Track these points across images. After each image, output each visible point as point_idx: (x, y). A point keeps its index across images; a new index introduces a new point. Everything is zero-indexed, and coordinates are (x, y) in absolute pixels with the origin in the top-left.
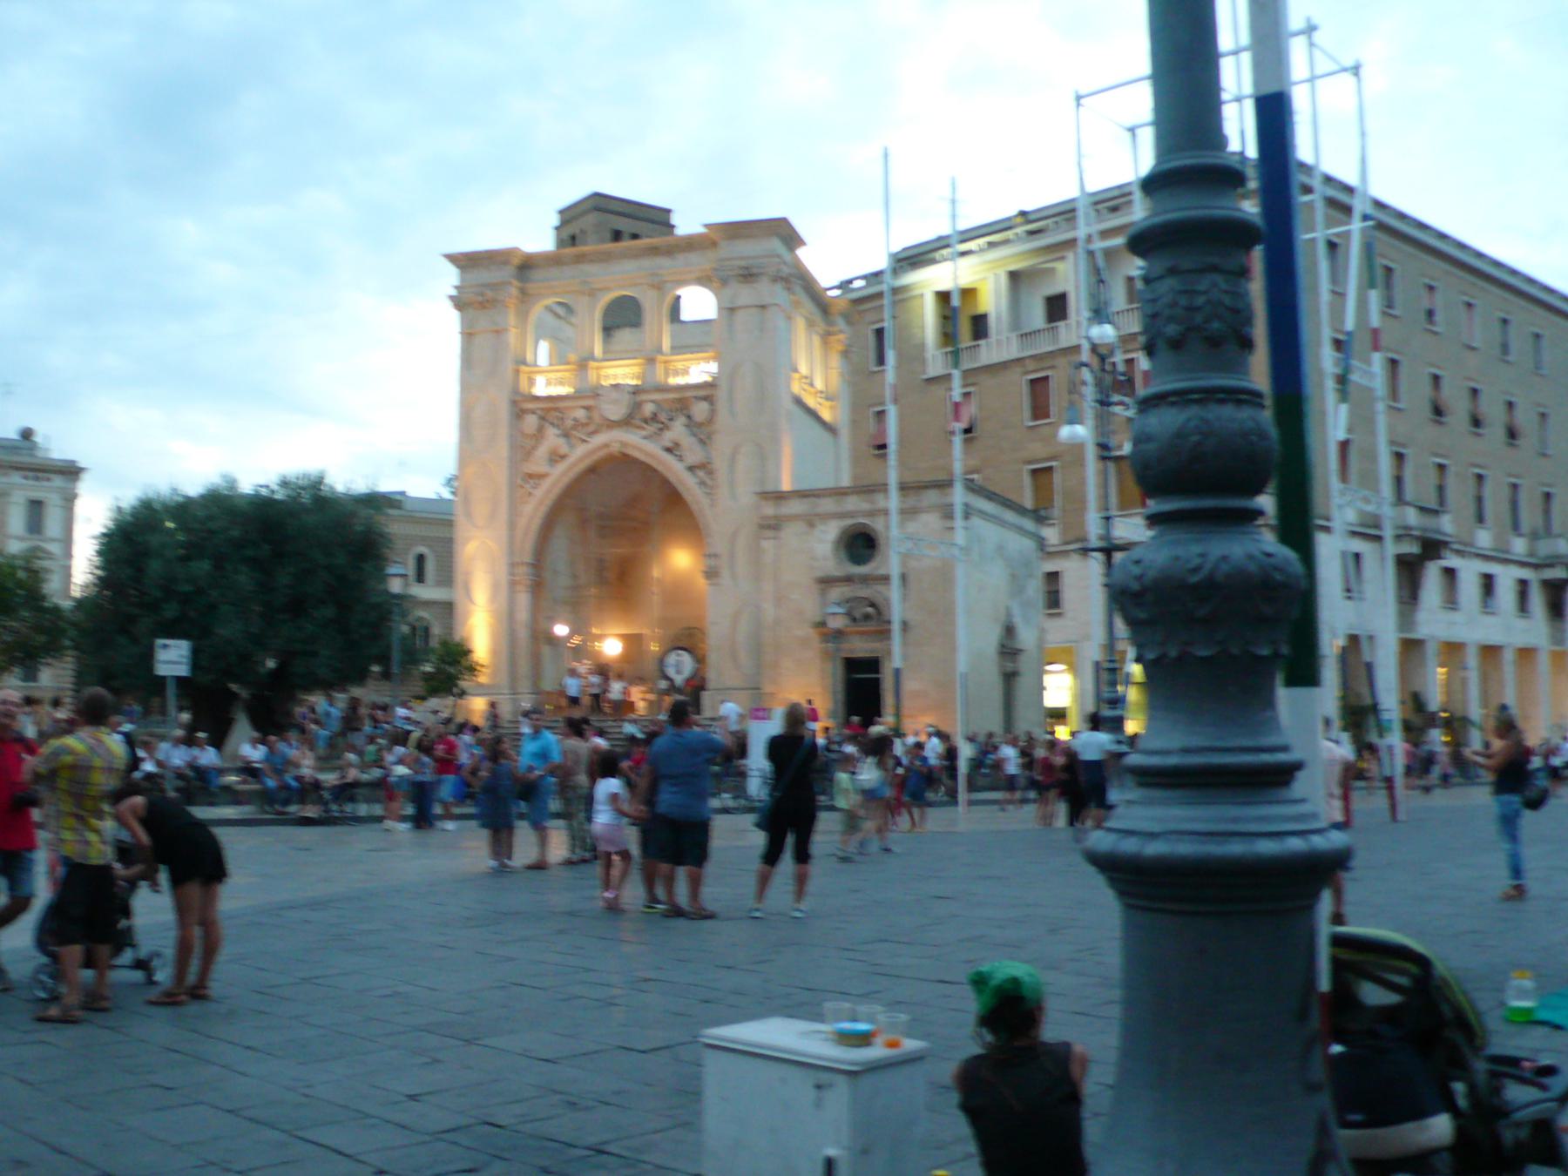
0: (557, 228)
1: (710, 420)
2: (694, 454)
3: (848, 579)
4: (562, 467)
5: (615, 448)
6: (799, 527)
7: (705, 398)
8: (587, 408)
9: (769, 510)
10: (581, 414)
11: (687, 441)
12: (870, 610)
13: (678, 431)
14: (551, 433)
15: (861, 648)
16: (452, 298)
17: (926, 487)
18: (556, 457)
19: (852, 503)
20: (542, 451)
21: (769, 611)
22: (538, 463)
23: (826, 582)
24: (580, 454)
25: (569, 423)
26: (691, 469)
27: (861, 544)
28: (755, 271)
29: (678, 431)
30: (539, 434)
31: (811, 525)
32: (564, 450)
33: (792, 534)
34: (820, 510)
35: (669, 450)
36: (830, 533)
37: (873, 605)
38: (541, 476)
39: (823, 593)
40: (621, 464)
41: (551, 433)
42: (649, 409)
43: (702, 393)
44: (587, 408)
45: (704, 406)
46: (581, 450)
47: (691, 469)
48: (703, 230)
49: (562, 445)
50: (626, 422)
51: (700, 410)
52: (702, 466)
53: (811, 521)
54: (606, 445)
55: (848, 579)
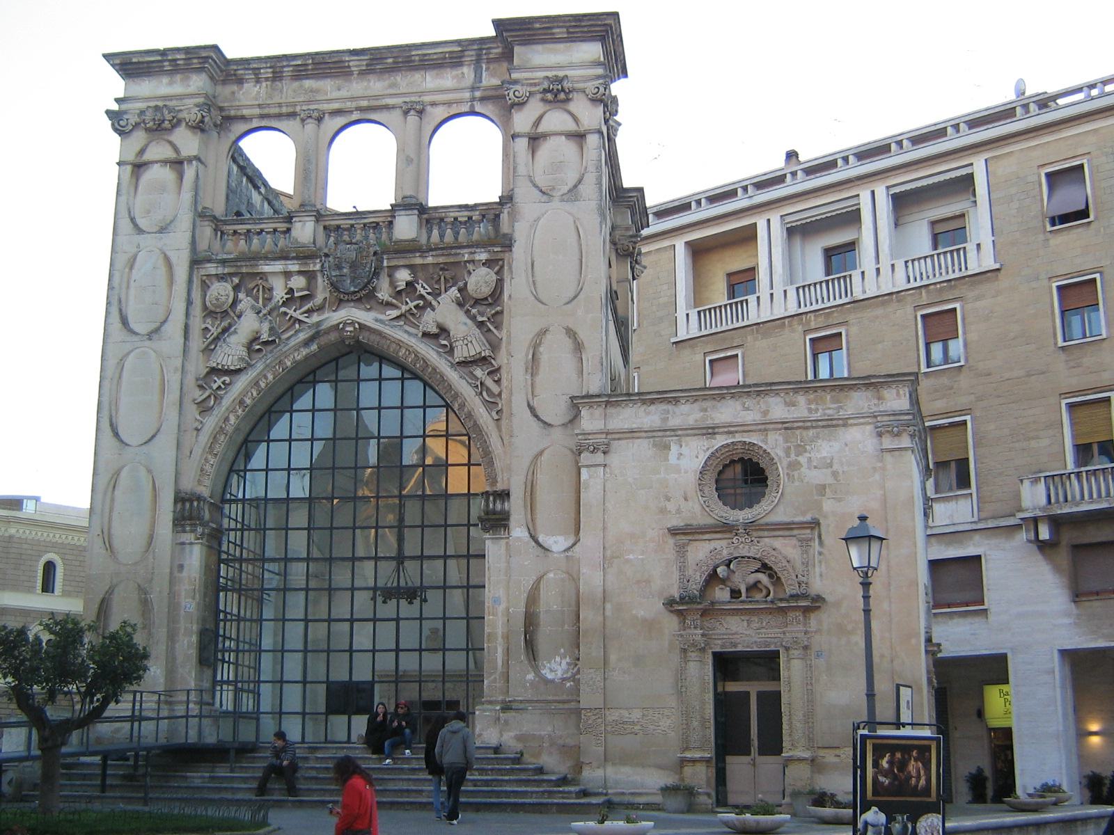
1: (496, 295)
3: (726, 528)
6: (642, 448)
9: (591, 421)
12: (763, 578)
15: (743, 634)
16: (109, 113)
17: (851, 387)
19: (727, 412)
21: (592, 579)
22: (231, 352)
23: (684, 533)
26: (465, 364)
27: (744, 475)
28: (566, 85)
33: (630, 458)
34: (674, 422)
36: (691, 457)
37: (765, 568)
39: (681, 550)
48: (491, 32)
51: (480, 280)
52: (482, 361)
53: (662, 437)
55: (726, 528)
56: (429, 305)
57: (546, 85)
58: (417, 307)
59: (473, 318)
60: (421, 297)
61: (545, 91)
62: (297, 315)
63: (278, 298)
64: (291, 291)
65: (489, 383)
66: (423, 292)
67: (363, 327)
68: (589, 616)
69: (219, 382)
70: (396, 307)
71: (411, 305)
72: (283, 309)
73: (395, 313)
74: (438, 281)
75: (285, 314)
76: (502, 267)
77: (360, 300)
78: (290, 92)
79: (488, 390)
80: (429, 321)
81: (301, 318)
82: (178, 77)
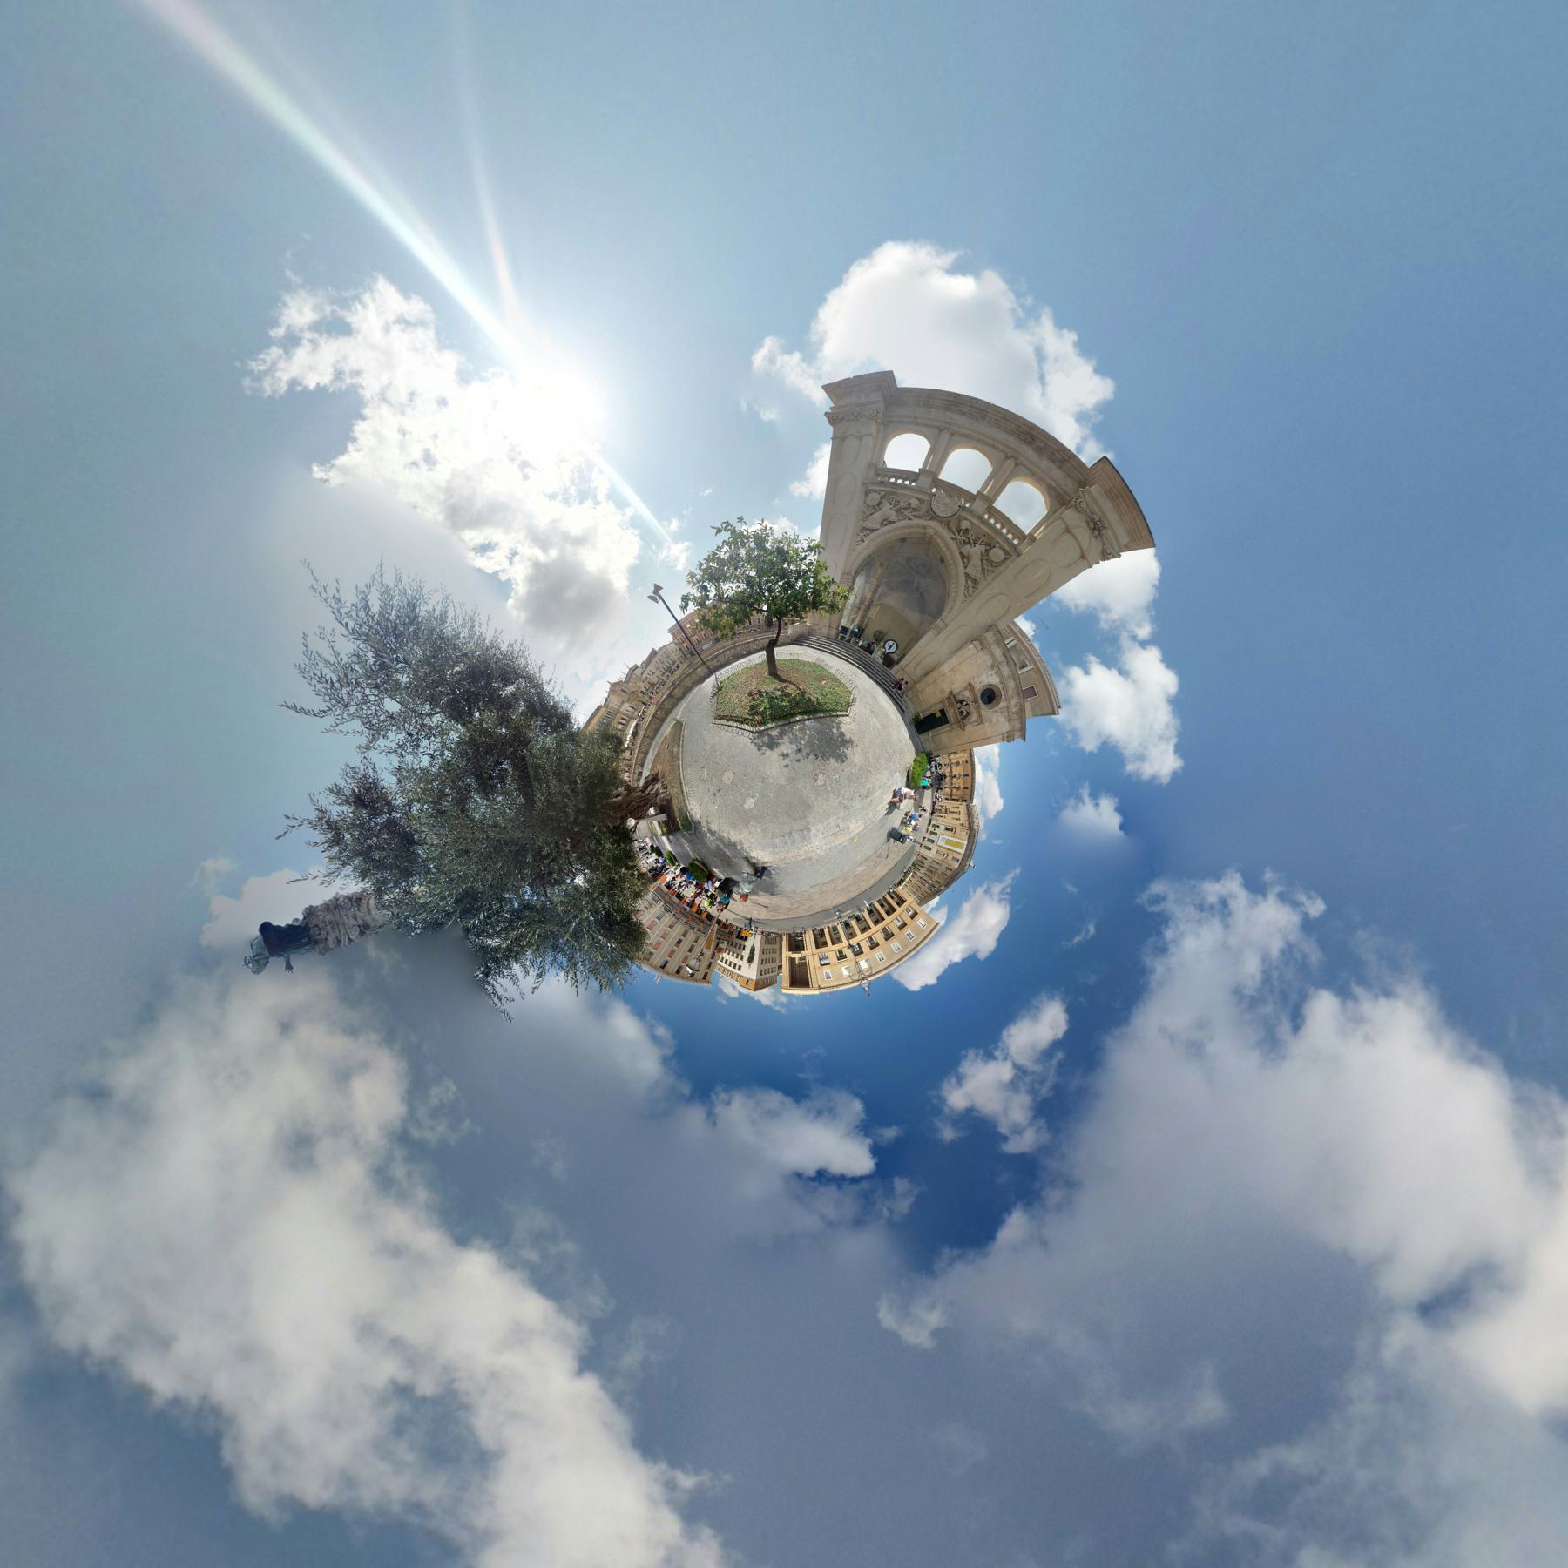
2: (975, 571)
7: (1006, 552)
8: (921, 501)
10: (914, 503)
11: (976, 560)
13: (976, 551)
14: (886, 507)
21: (945, 668)
24: (902, 526)
25: (903, 504)
26: (967, 576)
29: (976, 551)
31: (992, 667)
33: (984, 658)
35: (963, 556)
36: (990, 679)
40: (927, 542)
41: (886, 507)
42: (965, 525)
44: (921, 501)
45: (1001, 555)
47: (967, 576)
49: (893, 516)
50: (945, 521)
52: (974, 581)
68: (935, 673)
80: (967, 549)
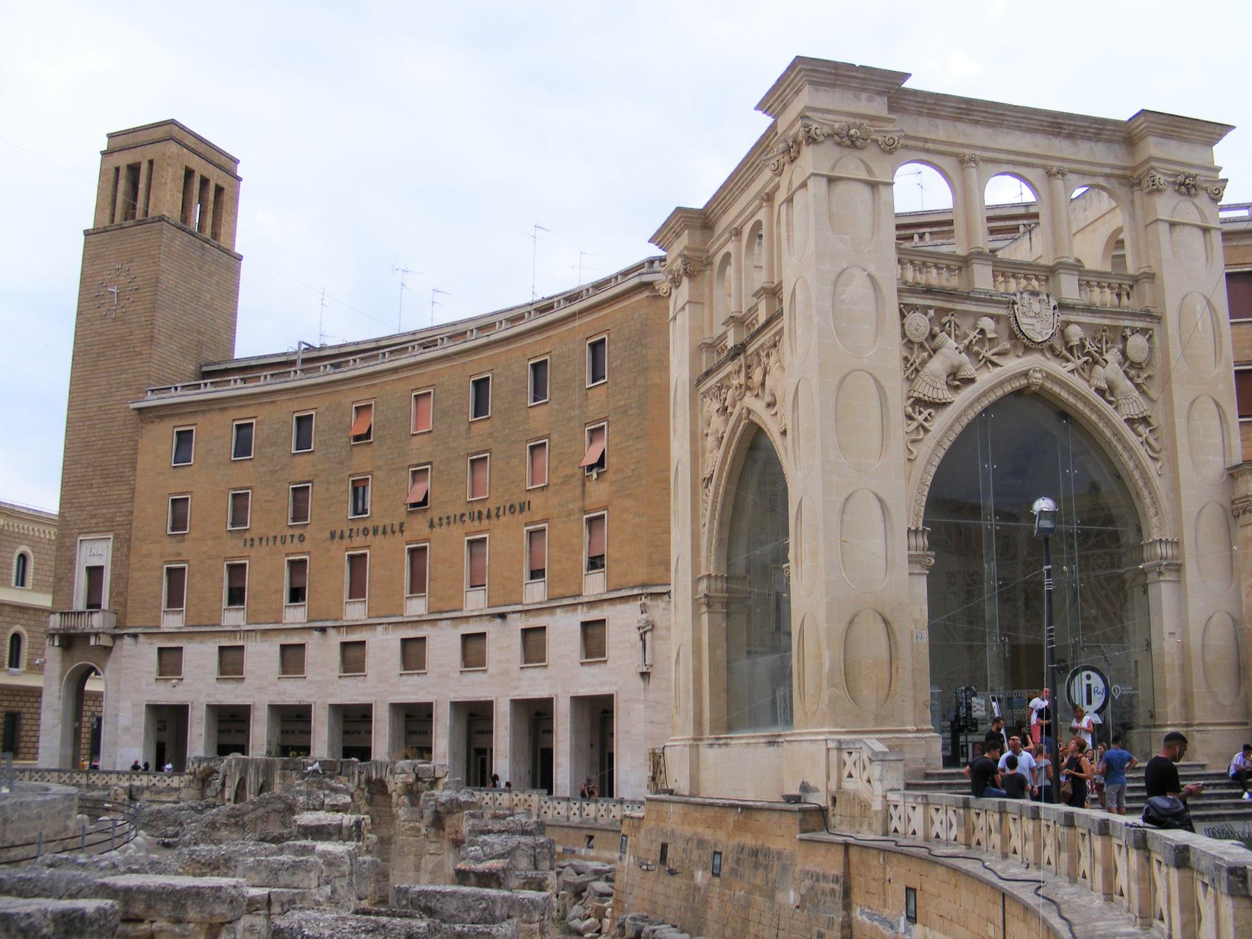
0: (103, 153)
4: (968, 393)
5: (1037, 378)
7: (1144, 331)
10: (987, 324)
18: (957, 380)
20: (937, 366)
26: (1130, 421)
30: (930, 345)
32: (969, 370)
38: (941, 405)
43: (1139, 324)
46: (985, 378)
52: (1145, 420)
54: (1025, 374)
56: (1096, 362)
57: (1180, 179)
58: (1086, 362)
59: (1131, 380)
60: (1088, 354)
61: (1181, 184)
62: (989, 354)
63: (971, 337)
64: (982, 331)
65: (1151, 441)
66: (1092, 350)
67: (1048, 376)
69: (926, 413)
70: (1068, 361)
71: (1079, 362)
72: (976, 348)
73: (1070, 366)
74: (1100, 341)
75: (978, 354)
76: (1151, 336)
77: (1042, 351)
78: (941, 131)
79: (1150, 446)
81: (994, 359)
82: (864, 96)
